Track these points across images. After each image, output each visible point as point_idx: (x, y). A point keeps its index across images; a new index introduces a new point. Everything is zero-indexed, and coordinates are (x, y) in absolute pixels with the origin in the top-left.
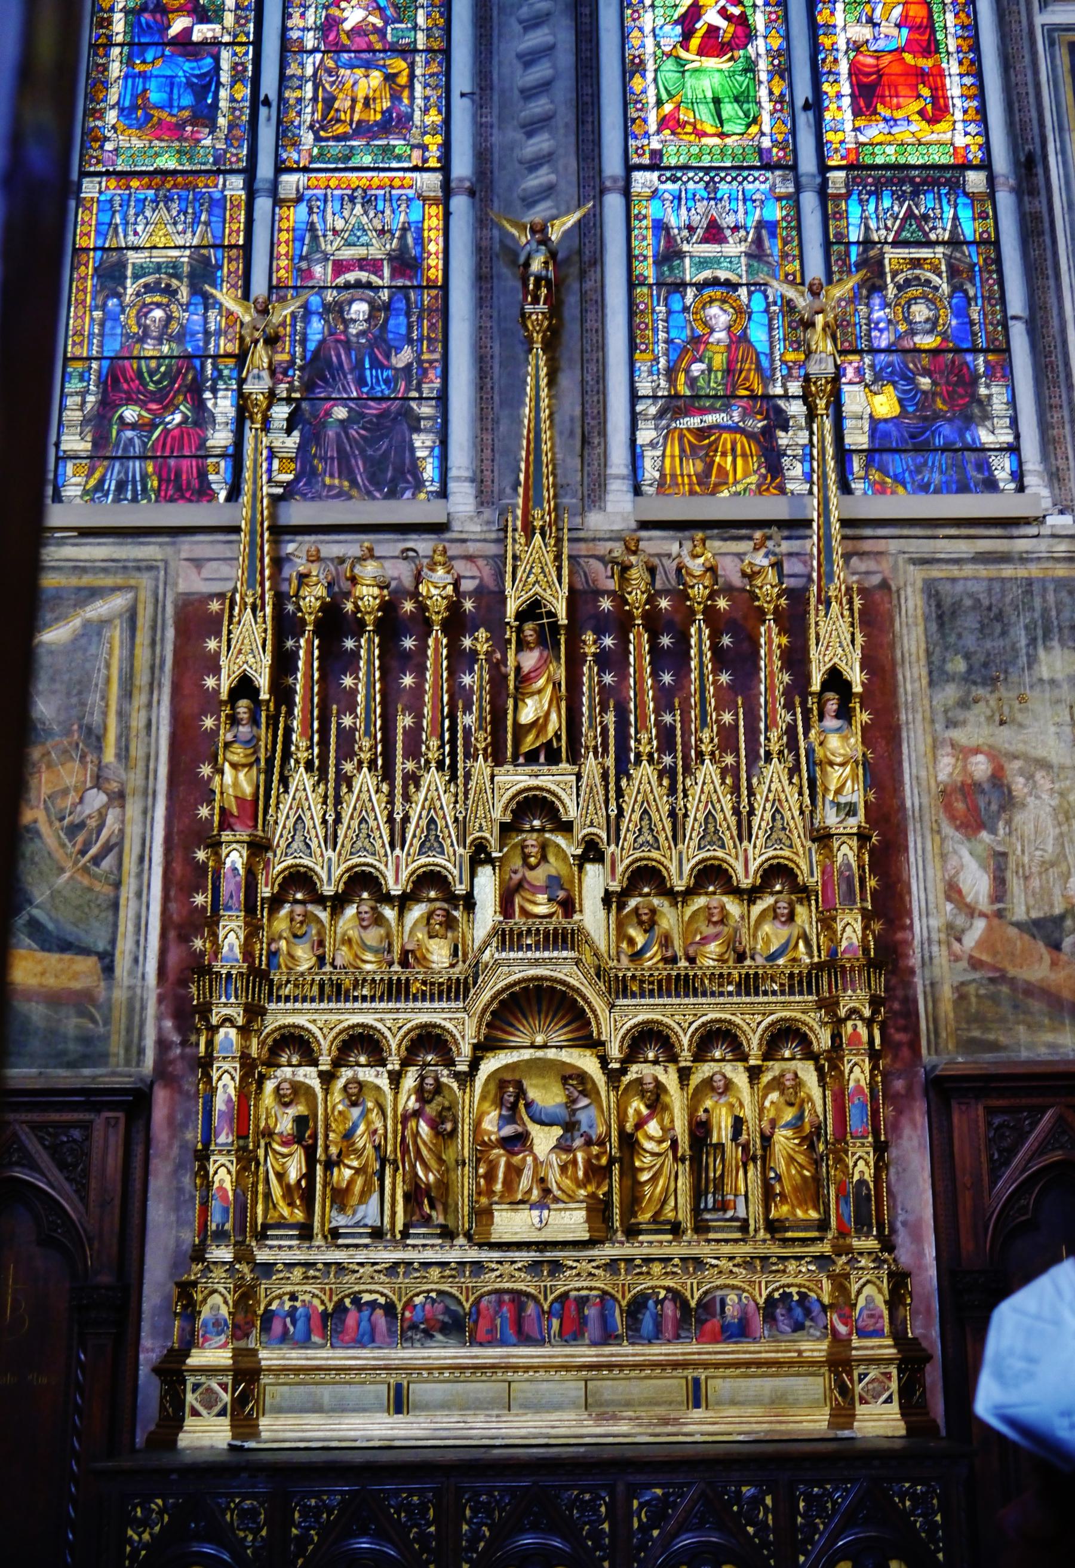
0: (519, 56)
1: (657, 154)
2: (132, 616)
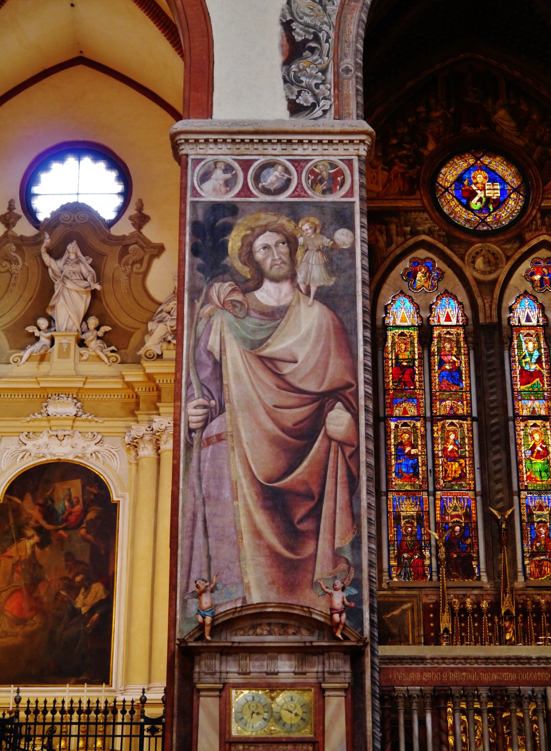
0: (493, 462)
1: (526, 486)
2: (412, 608)
